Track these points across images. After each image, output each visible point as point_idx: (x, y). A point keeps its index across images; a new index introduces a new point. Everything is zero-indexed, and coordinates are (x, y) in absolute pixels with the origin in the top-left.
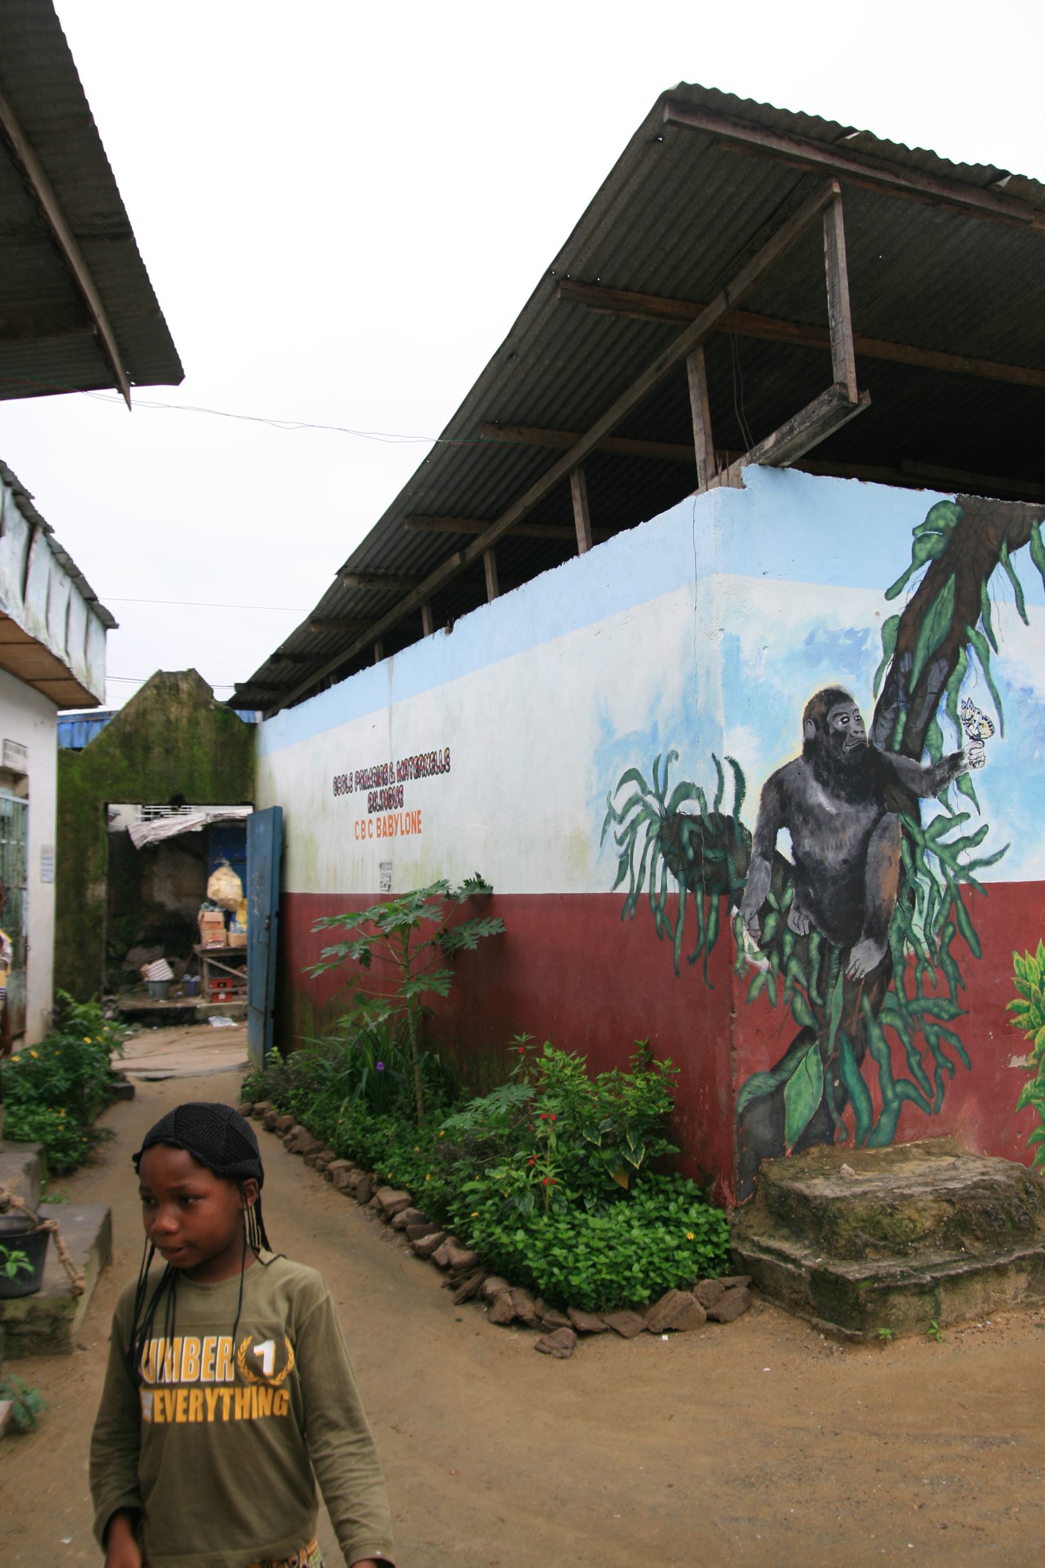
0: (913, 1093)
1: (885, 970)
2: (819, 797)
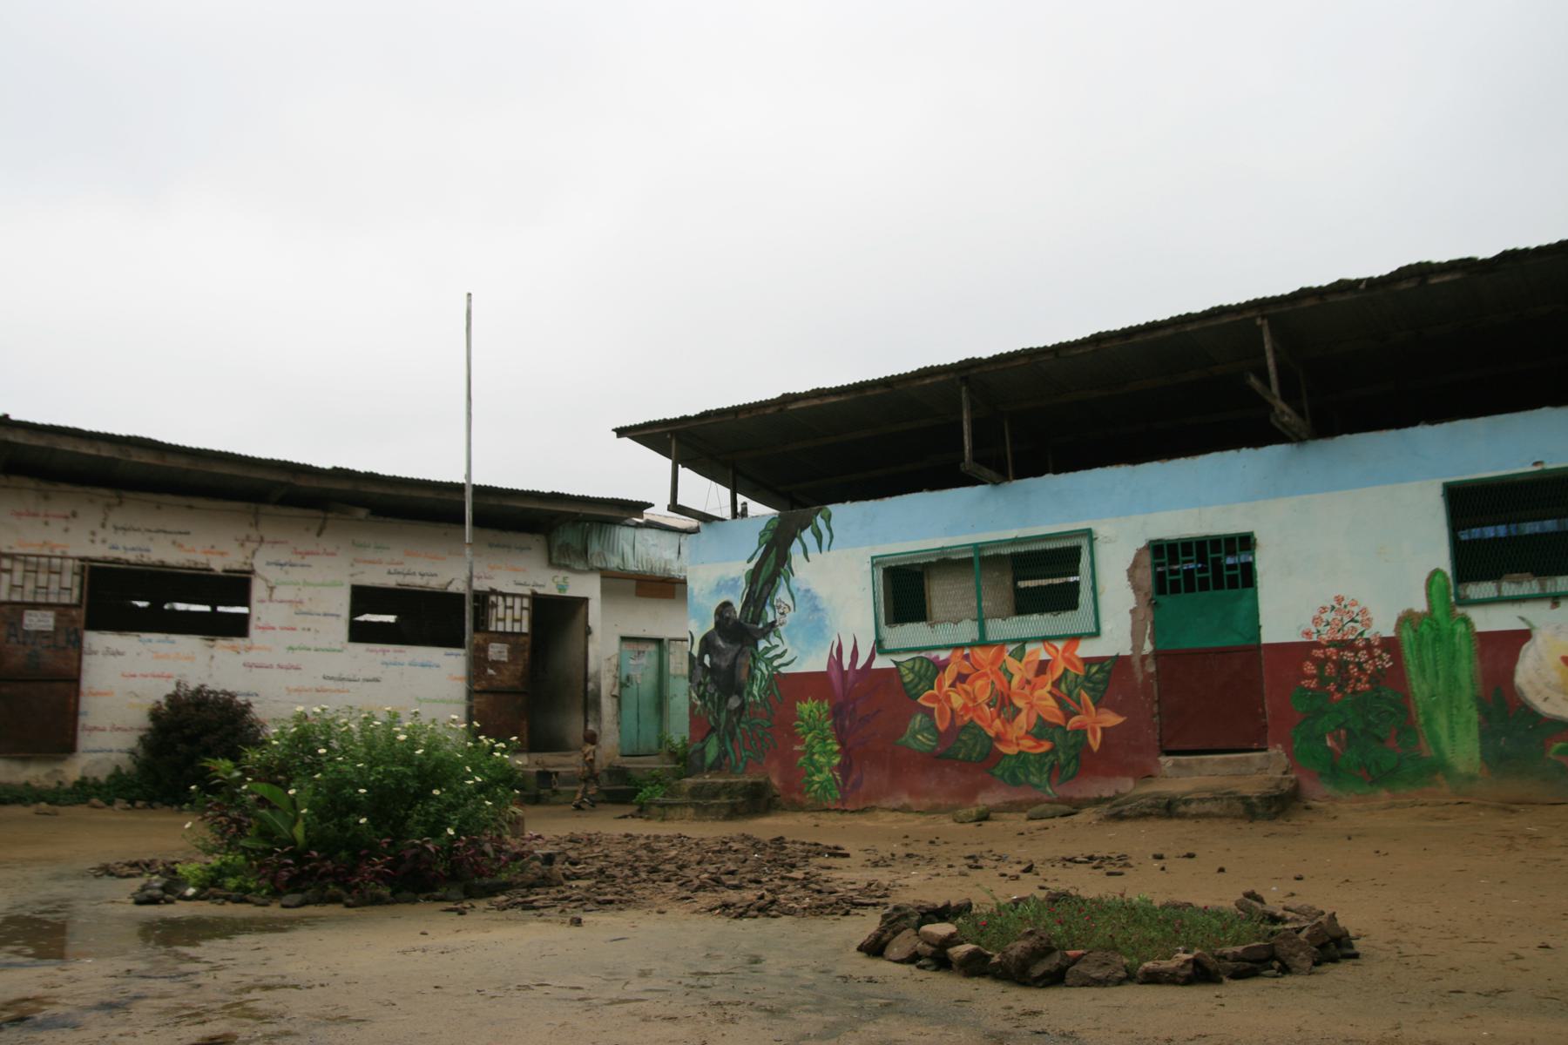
1: (742, 708)
2: (720, 643)
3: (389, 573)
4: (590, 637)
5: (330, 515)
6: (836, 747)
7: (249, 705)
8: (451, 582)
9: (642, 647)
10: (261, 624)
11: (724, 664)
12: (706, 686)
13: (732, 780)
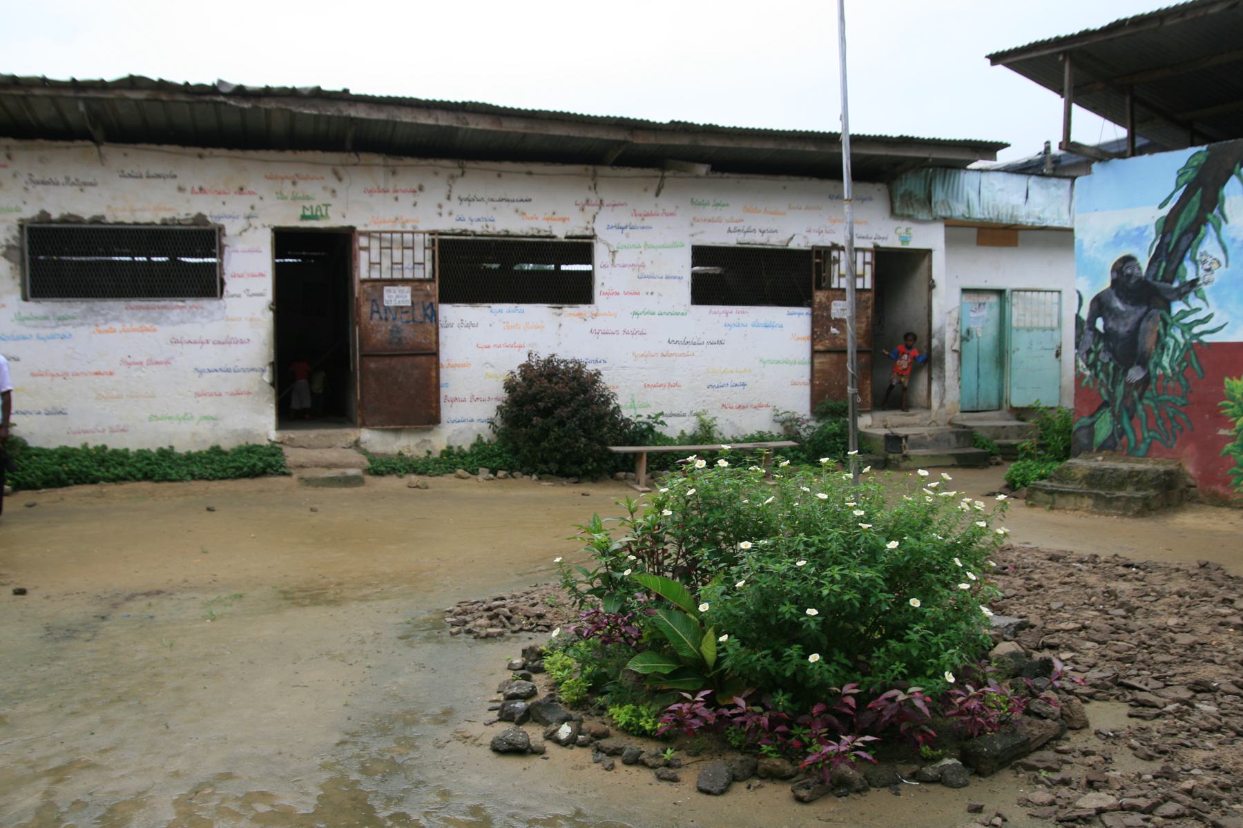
0: (1158, 436)
1: (1146, 381)
2: (1118, 304)
3: (729, 231)
4: (934, 291)
5: (667, 174)
7: (598, 373)
8: (792, 238)
9: (982, 299)
10: (605, 290)
11: (1123, 329)
12: (1097, 354)
13: (1139, 467)
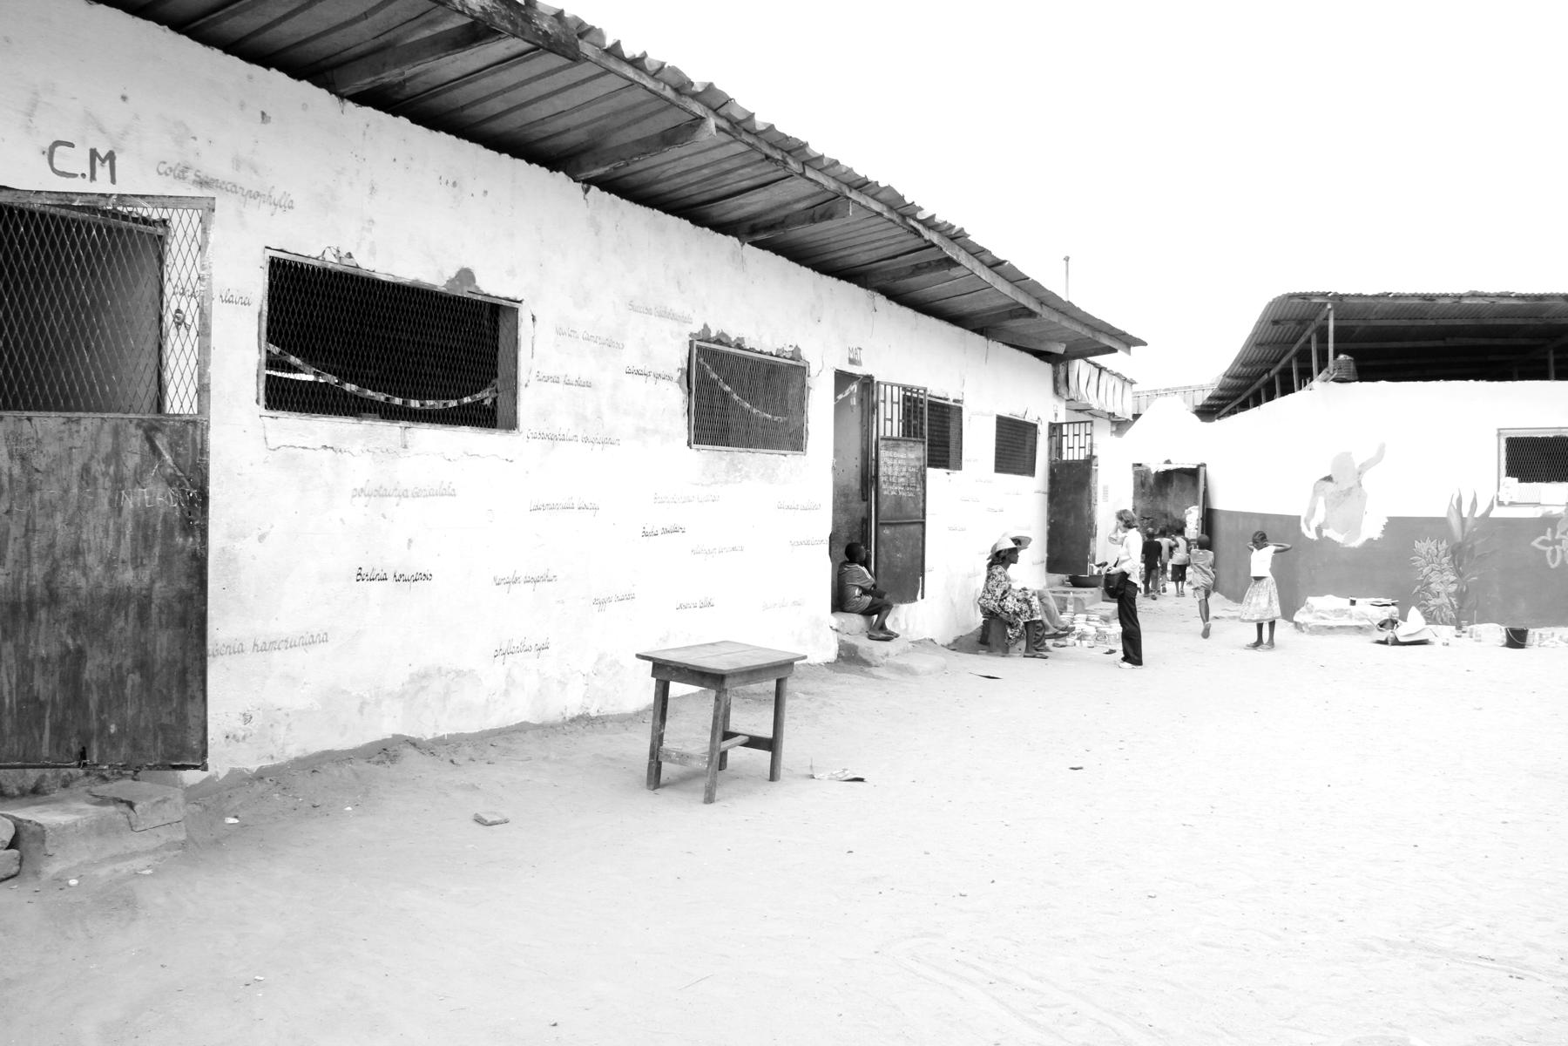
6: (1453, 578)
